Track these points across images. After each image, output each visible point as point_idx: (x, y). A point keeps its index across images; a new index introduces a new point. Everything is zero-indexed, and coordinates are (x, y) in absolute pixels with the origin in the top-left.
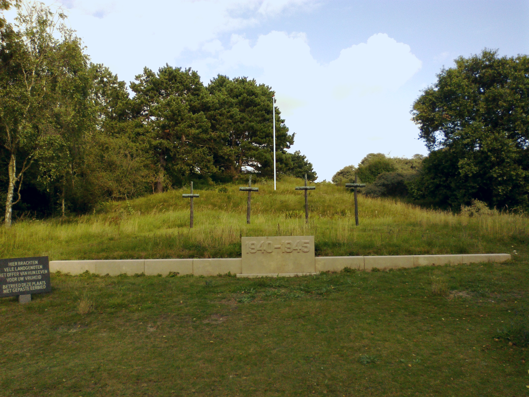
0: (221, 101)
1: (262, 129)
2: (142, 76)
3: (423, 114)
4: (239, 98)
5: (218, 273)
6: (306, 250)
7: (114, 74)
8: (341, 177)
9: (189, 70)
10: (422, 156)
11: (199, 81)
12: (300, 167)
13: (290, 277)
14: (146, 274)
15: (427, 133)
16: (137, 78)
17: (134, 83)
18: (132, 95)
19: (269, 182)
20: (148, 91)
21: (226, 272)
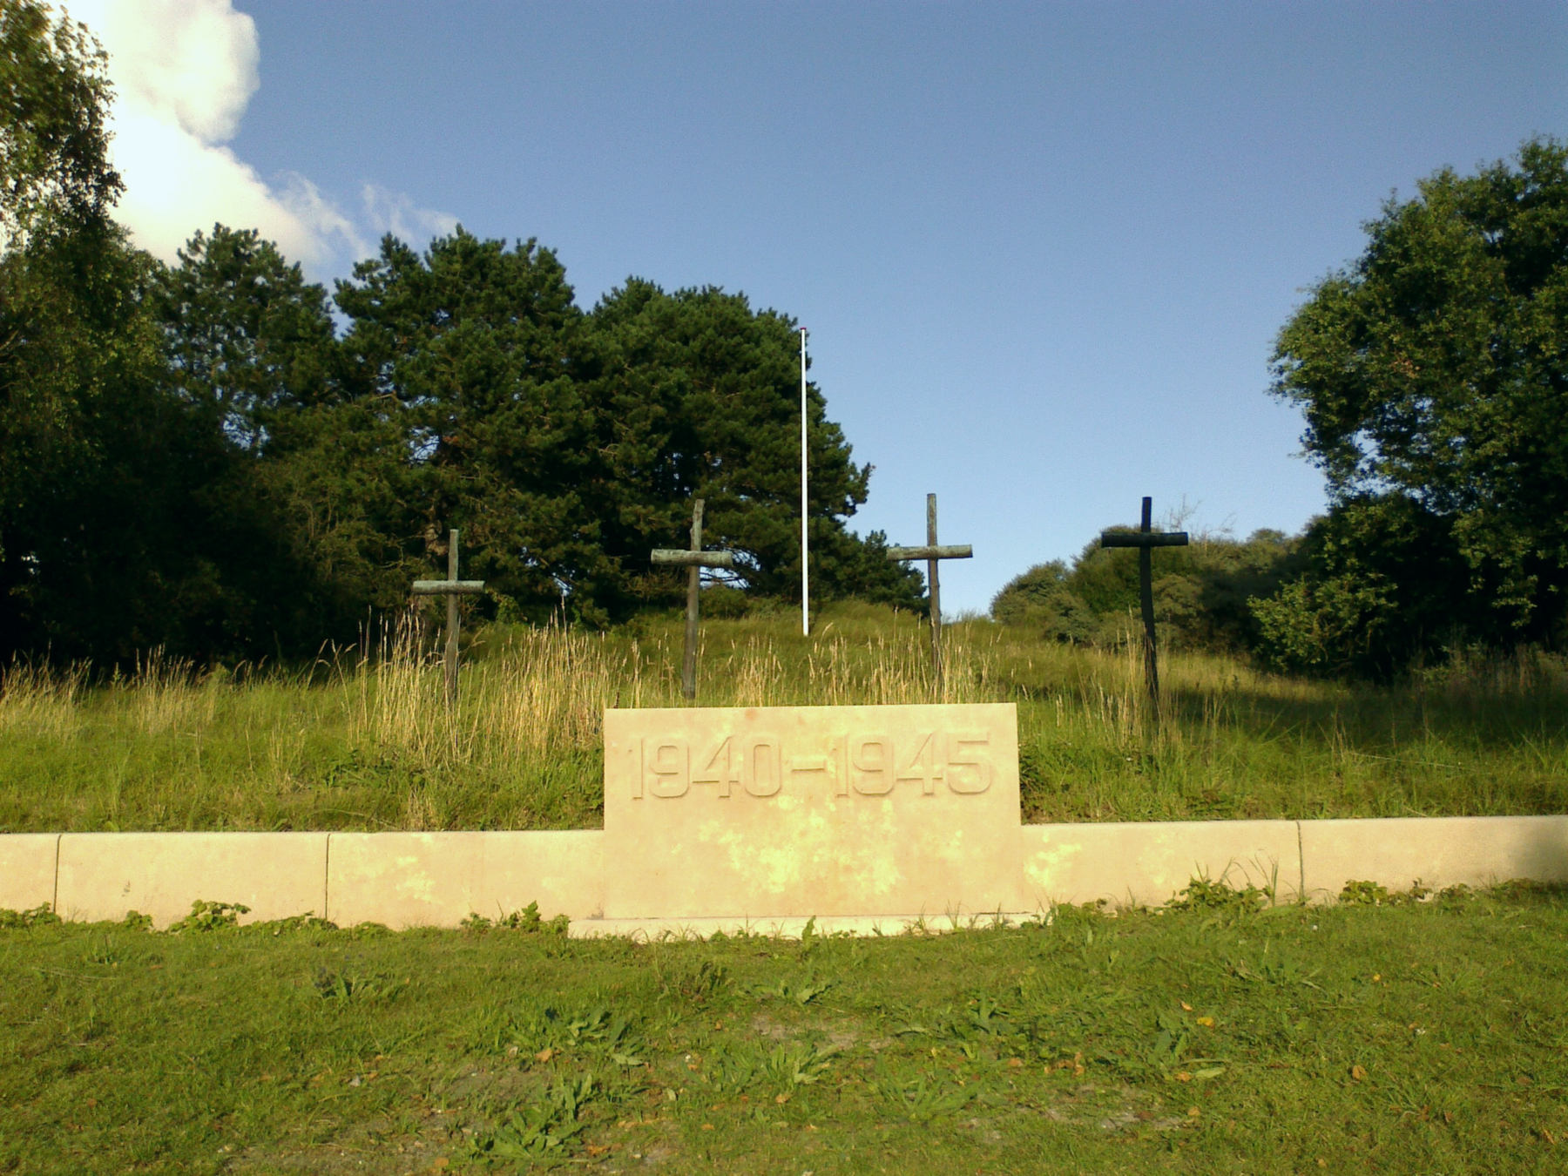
0: (631, 344)
1: (764, 443)
2: (378, 266)
3: (1322, 363)
5: (466, 915)
6: (968, 779)
7: (289, 263)
8: (1019, 597)
9: (531, 247)
10: (1280, 535)
11: (559, 280)
12: (885, 583)
13: (880, 939)
14: (64, 913)
15: (1328, 439)
17: (347, 284)
18: (343, 324)
19: (787, 611)
20: (397, 309)
21: (516, 906)
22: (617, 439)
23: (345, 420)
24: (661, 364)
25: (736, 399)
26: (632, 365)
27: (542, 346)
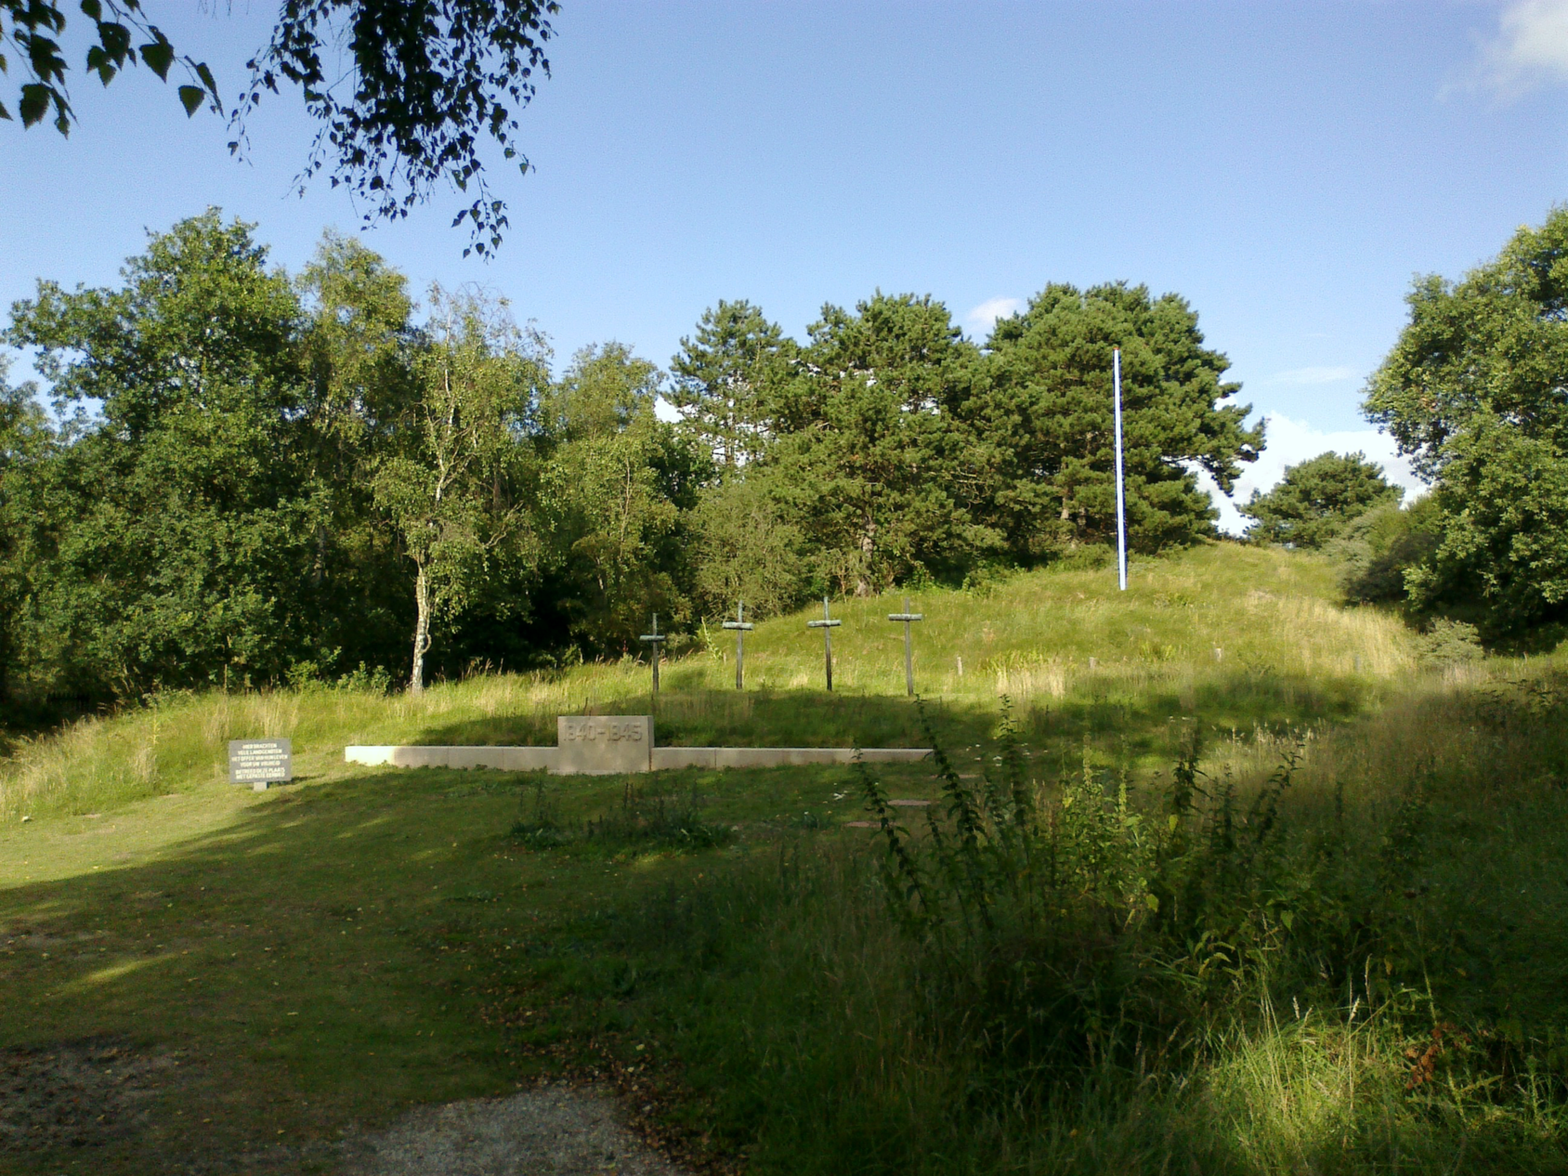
7: (770, 323)
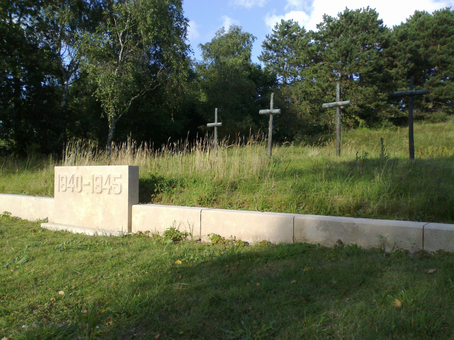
2: (323, 24)
4: (429, 30)
7: (301, 27)
16: (318, 26)
22: (396, 66)
23: (311, 71)
24: (410, 40)
25: (445, 47)
26: (401, 41)
27: (368, 40)
